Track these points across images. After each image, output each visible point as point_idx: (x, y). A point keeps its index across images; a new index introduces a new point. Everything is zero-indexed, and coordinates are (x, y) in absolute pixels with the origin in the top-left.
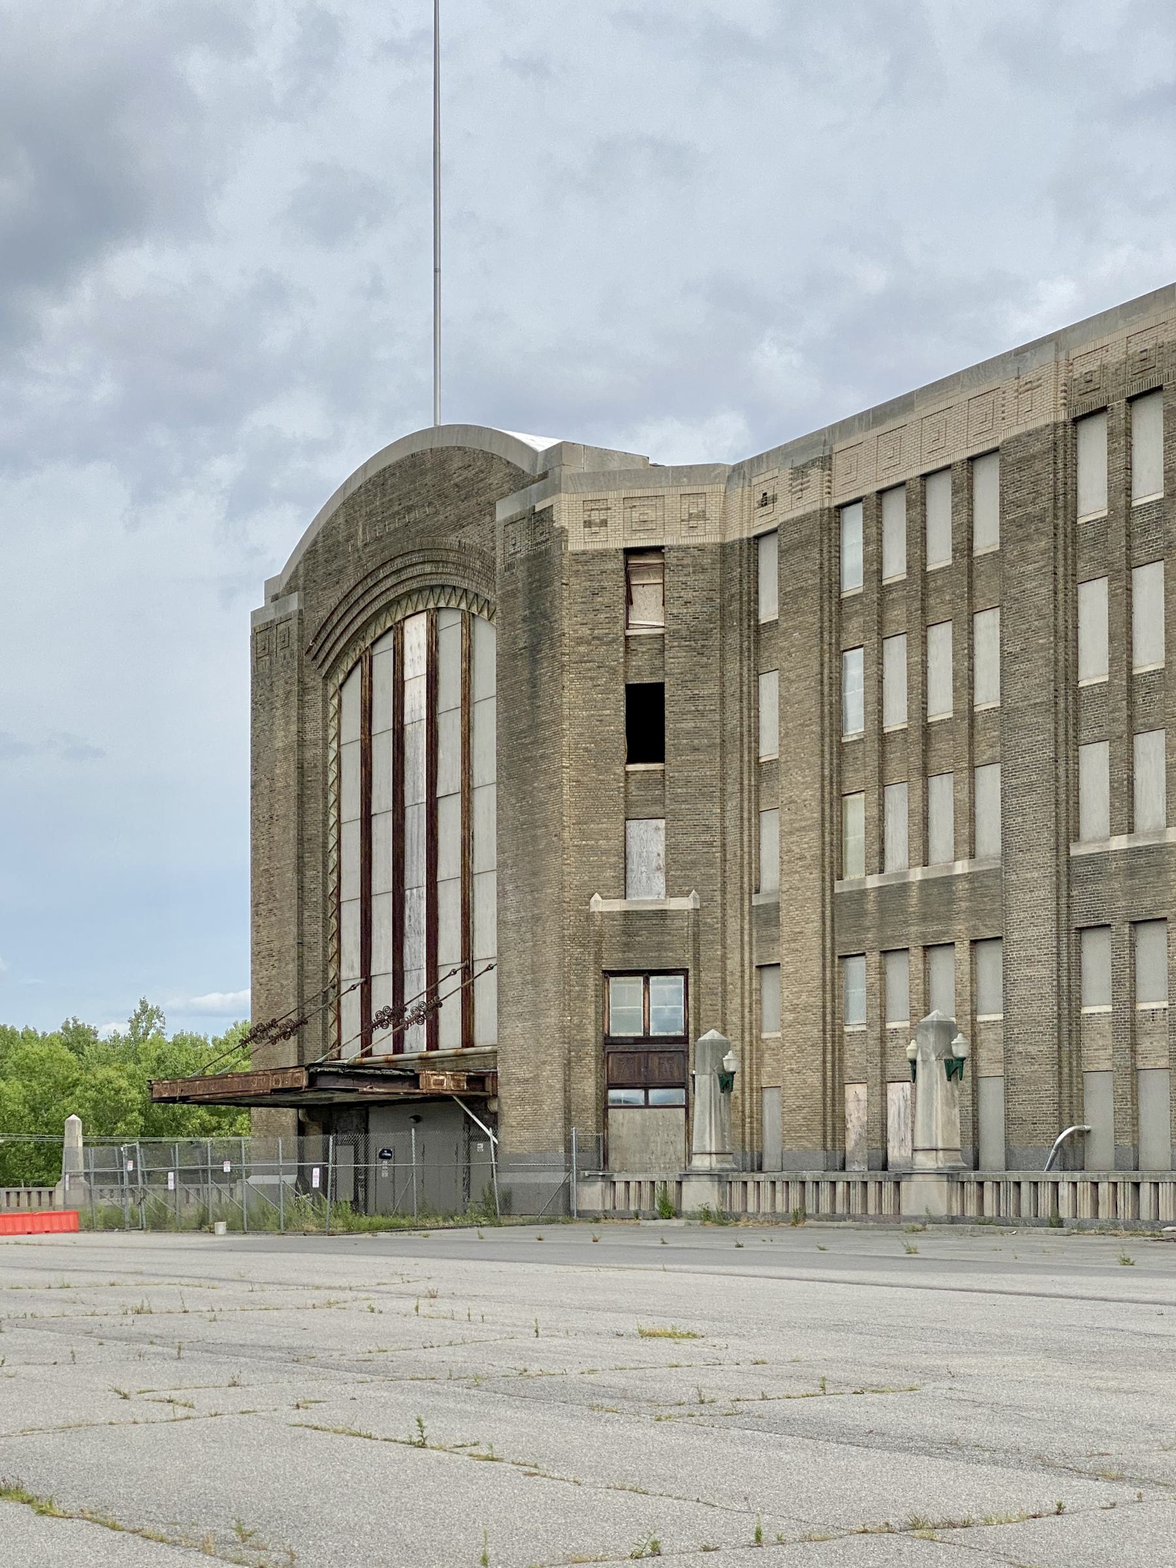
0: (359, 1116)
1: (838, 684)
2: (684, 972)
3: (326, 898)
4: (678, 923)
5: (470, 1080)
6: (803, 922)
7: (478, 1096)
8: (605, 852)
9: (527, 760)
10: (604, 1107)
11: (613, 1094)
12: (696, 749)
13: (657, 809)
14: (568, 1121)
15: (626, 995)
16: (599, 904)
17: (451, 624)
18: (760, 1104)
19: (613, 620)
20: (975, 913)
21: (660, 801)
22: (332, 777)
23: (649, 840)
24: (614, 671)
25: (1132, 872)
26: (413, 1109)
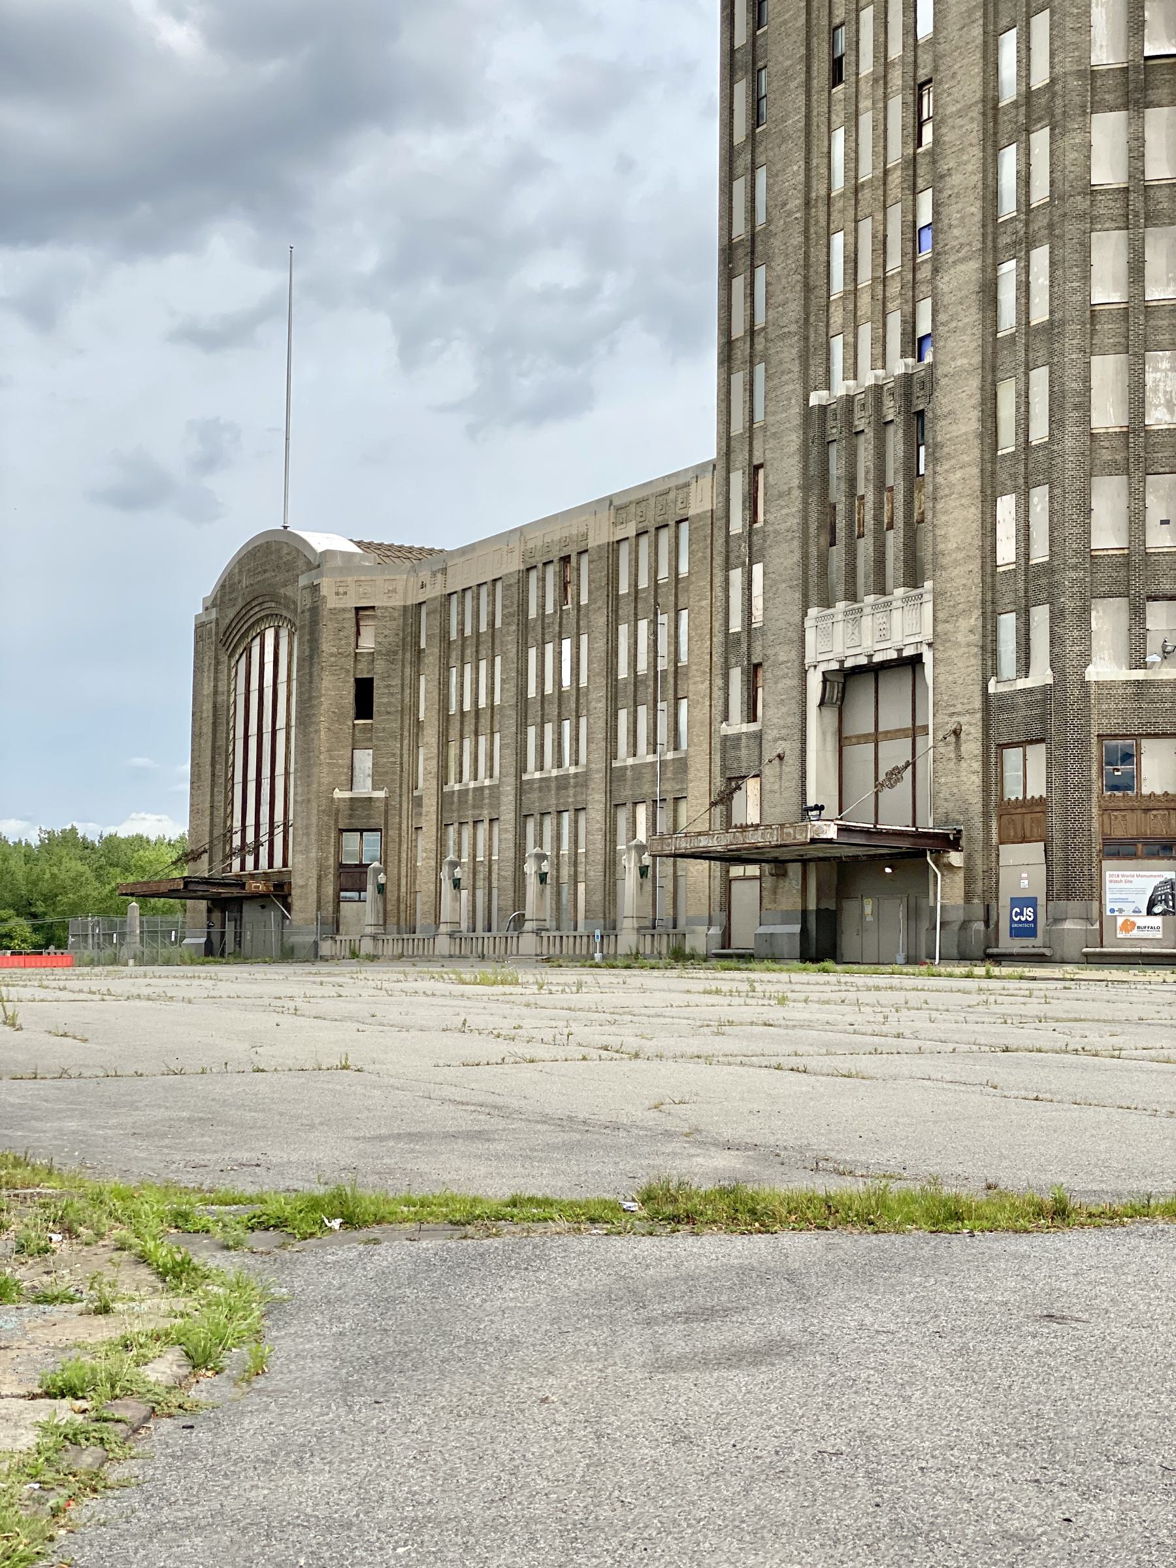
0: (227, 907)
1: (447, 684)
2: (380, 830)
3: (226, 781)
4: (378, 804)
5: (275, 886)
6: (430, 805)
7: (279, 892)
8: (342, 766)
9: (307, 716)
10: (338, 901)
11: (343, 894)
12: (388, 713)
13: (368, 744)
14: (319, 908)
15: (351, 841)
16: (338, 794)
17: (284, 633)
18: (415, 899)
19: (349, 644)
20: (491, 806)
21: (370, 740)
22: (232, 712)
23: (364, 760)
24: (348, 671)
25: (540, 789)
26: (261, 901)
